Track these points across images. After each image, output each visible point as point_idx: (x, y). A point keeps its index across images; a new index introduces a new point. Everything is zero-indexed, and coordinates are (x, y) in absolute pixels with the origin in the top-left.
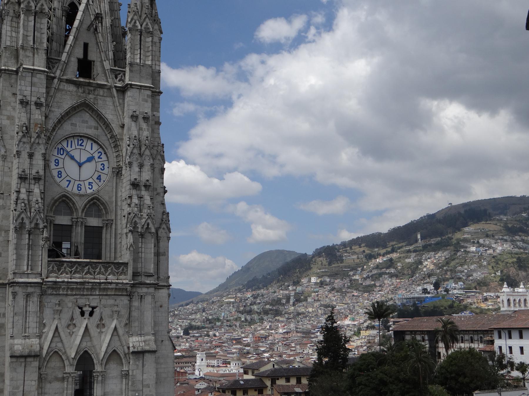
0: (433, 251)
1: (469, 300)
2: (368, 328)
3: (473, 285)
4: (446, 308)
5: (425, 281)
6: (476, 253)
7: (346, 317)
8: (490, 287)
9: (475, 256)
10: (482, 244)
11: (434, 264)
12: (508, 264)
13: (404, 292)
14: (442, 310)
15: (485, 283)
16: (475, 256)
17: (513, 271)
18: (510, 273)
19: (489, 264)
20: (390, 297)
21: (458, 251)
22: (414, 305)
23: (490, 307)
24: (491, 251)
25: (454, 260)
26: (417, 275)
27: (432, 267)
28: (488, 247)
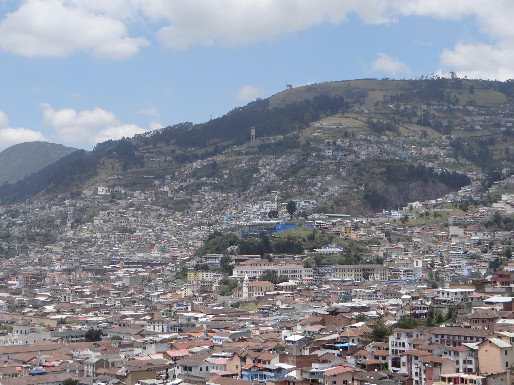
0: (273, 155)
1: (335, 229)
2: (197, 268)
3: (329, 204)
4: (304, 240)
5: (264, 197)
6: (333, 159)
7: (152, 246)
8: (351, 206)
9: (331, 163)
10: (340, 147)
11: (277, 173)
12: (375, 176)
13: (234, 212)
14: (299, 242)
15: (345, 201)
16: (331, 163)
17: (379, 186)
18: (378, 188)
19: (349, 175)
20: (214, 218)
21: (308, 155)
22: (262, 235)
23: (363, 238)
24: (352, 157)
25: (303, 167)
26: (252, 188)
27: (273, 176)
28: (348, 150)
